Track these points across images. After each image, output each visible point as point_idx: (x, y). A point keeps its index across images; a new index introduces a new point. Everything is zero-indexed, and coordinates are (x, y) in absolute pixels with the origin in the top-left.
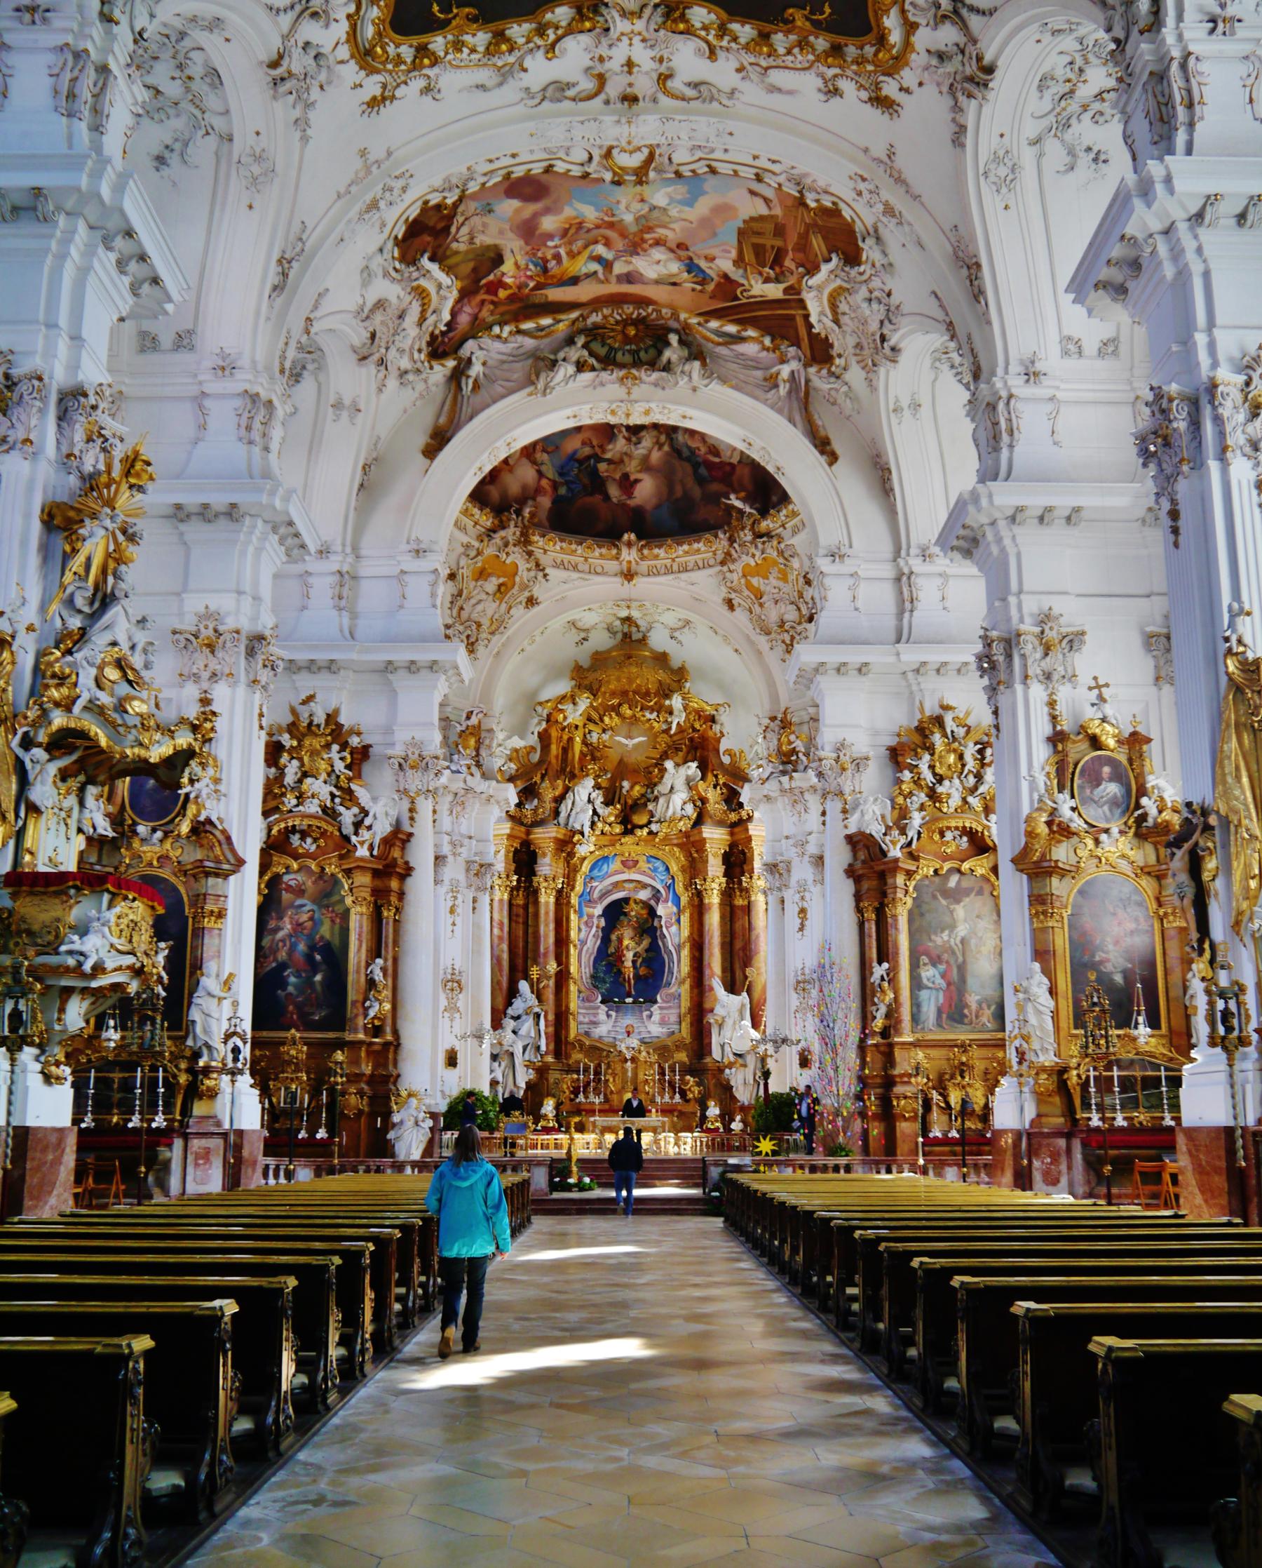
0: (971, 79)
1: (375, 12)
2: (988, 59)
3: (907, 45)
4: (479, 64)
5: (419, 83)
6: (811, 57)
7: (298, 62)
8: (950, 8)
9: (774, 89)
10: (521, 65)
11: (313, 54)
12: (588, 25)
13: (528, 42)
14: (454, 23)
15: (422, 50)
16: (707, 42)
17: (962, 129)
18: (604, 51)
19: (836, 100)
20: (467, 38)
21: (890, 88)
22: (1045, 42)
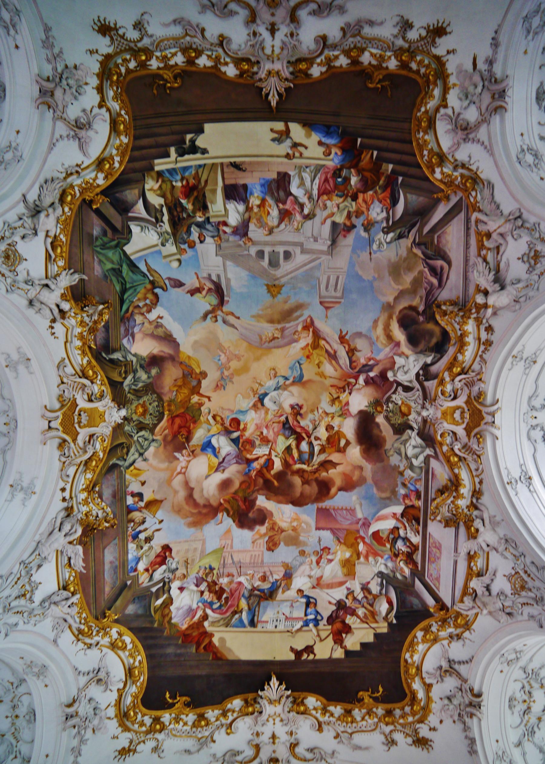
0: (471, 704)
1: (134, 689)
2: (476, 691)
3: (429, 699)
4: (189, 735)
5: (151, 744)
6: (376, 720)
7: (83, 708)
8: (448, 666)
9: (357, 748)
10: (212, 737)
11: (93, 704)
12: (250, 709)
13: (217, 720)
14: (177, 706)
15: (157, 720)
16: (317, 719)
17: (473, 741)
18: (259, 729)
19: (394, 748)
20: (183, 717)
21: (424, 731)
22: (505, 671)
